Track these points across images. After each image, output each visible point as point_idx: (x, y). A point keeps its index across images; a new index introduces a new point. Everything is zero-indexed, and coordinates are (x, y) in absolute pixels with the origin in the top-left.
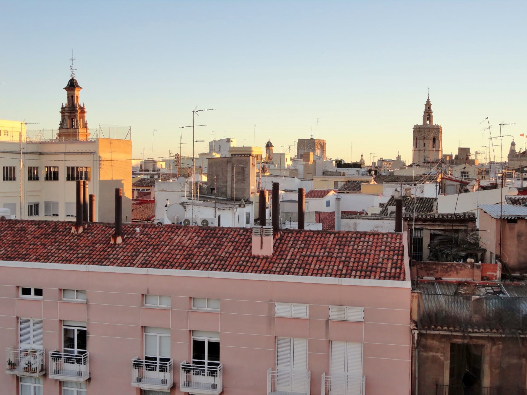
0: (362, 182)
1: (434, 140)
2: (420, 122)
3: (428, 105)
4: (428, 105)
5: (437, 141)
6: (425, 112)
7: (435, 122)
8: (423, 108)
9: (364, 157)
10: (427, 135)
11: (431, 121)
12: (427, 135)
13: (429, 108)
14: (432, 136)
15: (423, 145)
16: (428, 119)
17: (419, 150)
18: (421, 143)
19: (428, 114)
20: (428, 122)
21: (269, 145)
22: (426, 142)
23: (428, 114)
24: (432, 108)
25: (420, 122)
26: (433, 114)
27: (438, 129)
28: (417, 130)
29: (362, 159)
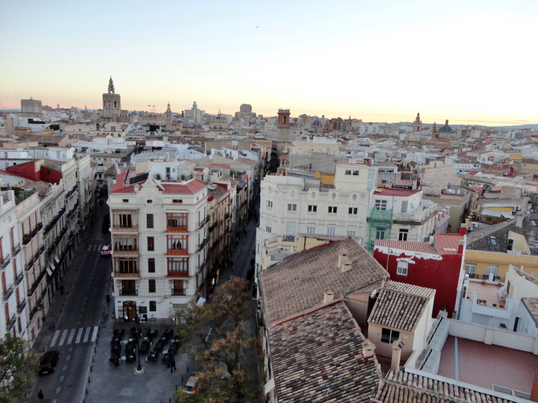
0: (7, 142)
1: (115, 103)
2: (107, 92)
3: (111, 81)
4: (111, 81)
7: (116, 92)
10: (111, 99)
11: (113, 92)
12: (111, 99)
14: (114, 100)
18: (107, 104)
19: (111, 87)
20: (111, 92)
22: (111, 104)
23: (111, 87)
25: (107, 92)
27: (118, 97)
28: (105, 96)
29: (86, 109)
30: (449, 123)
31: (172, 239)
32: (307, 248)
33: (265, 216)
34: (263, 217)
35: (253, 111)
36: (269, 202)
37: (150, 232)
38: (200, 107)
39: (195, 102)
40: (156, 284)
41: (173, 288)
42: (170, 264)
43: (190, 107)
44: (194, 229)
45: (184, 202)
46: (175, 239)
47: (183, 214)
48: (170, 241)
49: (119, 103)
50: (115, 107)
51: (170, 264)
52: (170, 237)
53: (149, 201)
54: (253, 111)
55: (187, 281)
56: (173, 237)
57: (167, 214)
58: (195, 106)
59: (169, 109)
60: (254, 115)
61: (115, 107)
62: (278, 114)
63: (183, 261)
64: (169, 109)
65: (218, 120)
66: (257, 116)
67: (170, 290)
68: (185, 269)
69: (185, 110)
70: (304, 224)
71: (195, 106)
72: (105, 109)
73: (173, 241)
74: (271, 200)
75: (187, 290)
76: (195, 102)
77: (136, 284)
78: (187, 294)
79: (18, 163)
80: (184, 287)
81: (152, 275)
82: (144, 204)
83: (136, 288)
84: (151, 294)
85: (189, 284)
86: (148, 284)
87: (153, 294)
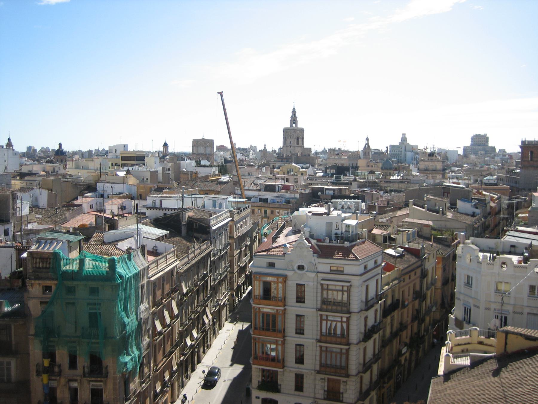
2: (288, 126)
3: (294, 112)
4: (294, 112)
5: (300, 140)
6: (292, 117)
7: (300, 126)
8: (291, 115)
9: (266, 146)
10: (293, 135)
11: (296, 125)
12: (293, 135)
13: (295, 115)
15: (289, 142)
16: (294, 123)
17: (287, 146)
18: (288, 141)
19: (294, 119)
20: (294, 125)
21: (165, 145)
22: (292, 140)
23: (294, 119)
24: (297, 115)
25: (288, 126)
26: (298, 119)
27: (302, 131)
28: (286, 131)
29: (265, 148)
30: (63, 147)
31: (327, 320)
32: (510, 349)
33: (462, 297)
34: (459, 299)
35: (491, 144)
36: (468, 277)
37: (300, 309)
38: (411, 141)
39: (404, 135)
40: (305, 381)
41: (326, 388)
42: (324, 354)
43: (396, 142)
44: (356, 310)
45: (345, 272)
46: (332, 321)
47: (343, 286)
48: (324, 323)
49: (303, 138)
50: (298, 144)
51: (324, 354)
52: (324, 317)
53: (301, 268)
54: (491, 144)
55: (346, 382)
56: (329, 318)
57: (322, 285)
58: (404, 139)
59: (367, 144)
60: (493, 149)
61: (298, 144)
62: (521, 147)
63: (341, 353)
64: (367, 144)
65: (430, 158)
66: (497, 151)
67: (322, 392)
68: (343, 364)
69: (391, 146)
70: (522, 313)
71: (404, 139)
72: (285, 148)
73: (329, 323)
74: (471, 274)
75: (345, 395)
76: (404, 135)
77: (279, 377)
78: (344, 400)
79: (169, 212)
80: (341, 391)
81: (300, 366)
82: (294, 270)
83: (279, 382)
84: (297, 393)
85: (348, 387)
86: (294, 379)
87: (301, 393)
